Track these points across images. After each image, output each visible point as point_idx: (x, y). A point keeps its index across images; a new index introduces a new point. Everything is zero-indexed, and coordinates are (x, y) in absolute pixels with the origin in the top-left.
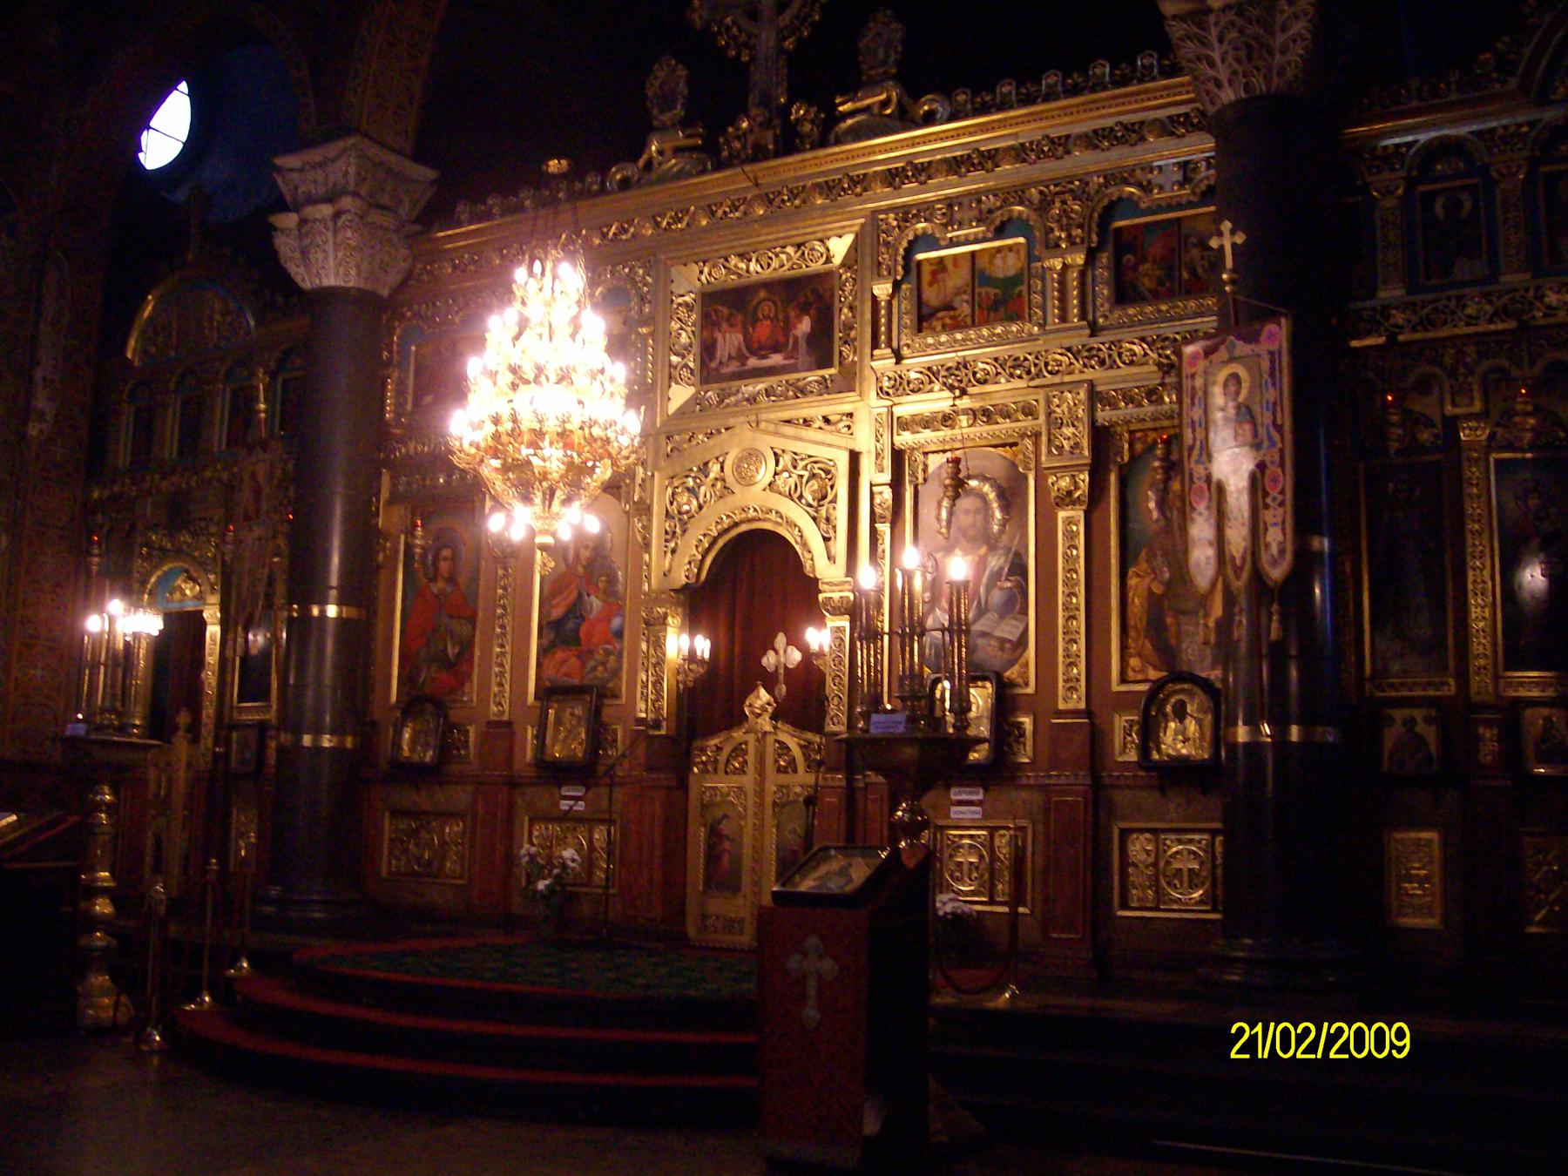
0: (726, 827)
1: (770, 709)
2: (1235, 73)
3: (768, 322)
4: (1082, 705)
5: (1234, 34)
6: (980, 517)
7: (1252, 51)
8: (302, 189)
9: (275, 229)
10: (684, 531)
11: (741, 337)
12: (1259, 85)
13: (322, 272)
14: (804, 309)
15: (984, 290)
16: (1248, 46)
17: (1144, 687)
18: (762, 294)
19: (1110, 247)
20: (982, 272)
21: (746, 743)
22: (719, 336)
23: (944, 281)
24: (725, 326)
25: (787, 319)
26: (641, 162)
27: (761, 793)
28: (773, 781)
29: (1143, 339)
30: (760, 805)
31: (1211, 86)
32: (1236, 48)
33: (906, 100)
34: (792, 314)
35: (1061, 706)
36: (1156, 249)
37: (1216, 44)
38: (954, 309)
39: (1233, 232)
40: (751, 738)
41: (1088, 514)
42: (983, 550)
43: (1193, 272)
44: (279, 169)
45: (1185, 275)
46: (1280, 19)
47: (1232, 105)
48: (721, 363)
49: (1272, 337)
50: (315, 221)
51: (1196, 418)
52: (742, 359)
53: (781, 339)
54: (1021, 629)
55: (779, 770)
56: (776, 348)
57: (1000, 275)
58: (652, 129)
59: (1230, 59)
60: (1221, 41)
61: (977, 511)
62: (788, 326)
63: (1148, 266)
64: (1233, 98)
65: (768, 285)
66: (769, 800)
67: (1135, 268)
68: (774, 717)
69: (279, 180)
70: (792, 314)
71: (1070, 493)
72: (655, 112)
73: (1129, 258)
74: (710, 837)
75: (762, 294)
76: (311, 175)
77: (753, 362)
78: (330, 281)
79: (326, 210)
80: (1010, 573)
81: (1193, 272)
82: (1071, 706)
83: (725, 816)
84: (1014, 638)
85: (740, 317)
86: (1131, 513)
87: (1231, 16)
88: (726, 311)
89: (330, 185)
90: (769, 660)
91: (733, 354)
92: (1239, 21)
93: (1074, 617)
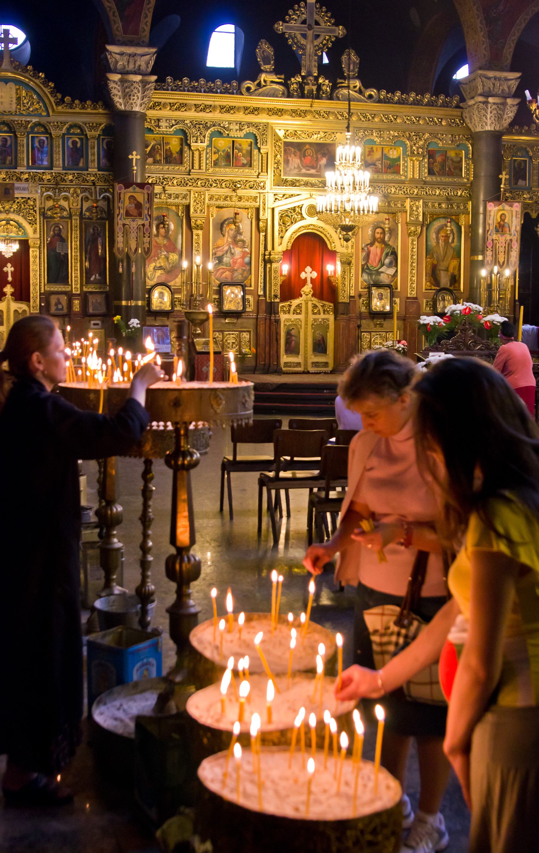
0: (293, 332)
1: (312, 293)
2: (493, 123)
3: (309, 157)
4: (415, 296)
5: (495, 112)
6: (382, 236)
7: (499, 118)
8: (120, 63)
9: (109, 80)
10: (287, 230)
11: (299, 161)
12: (497, 128)
13: (134, 105)
14: (324, 155)
15: (386, 161)
16: (499, 117)
17: (434, 291)
18: (307, 146)
19: (427, 156)
20: (385, 155)
21: (301, 304)
22: (290, 158)
23: (373, 155)
24: (293, 155)
25: (317, 158)
26: (256, 83)
27: (306, 321)
28: (311, 317)
29: (439, 188)
30: (306, 324)
31: (484, 124)
32: (495, 117)
33: (362, 88)
34: (319, 156)
35: (409, 296)
36: (439, 159)
37: (489, 113)
38: (376, 165)
39: (506, 175)
40: (303, 302)
41: (418, 238)
42: (383, 246)
43: (450, 169)
44: (108, 51)
45: (447, 169)
46: (506, 111)
47: (488, 131)
48: (291, 169)
49: (517, 206)
50: (134, 82)
51: (490, 223)
52: (300, 170)
53: (315, 165)
54: (395, 271)
55: (314, 314)
56: (313, 167)
57: (391, 157)
58: (262, 71)
59: (493, 118)
60: (491, 113)
61: (381, 233)
62: (317, 160)
63: (436, 164)
64: (489, 129)
65: (310, 144)
66: (310, 323)
67: (433, 164)
68: (313, 295)
69: (109, 57)
70: (319, 156)
71: (414, 232)
72: (262, 63)
73: (431, 160)
74: (287, 336)
75: (307, 146)
76: (126, 58)
77: (304, 171)
78: (137, 109)
79: (138, 78)
80: (392, 254)
81: (450, 169)
82: (411, 296)
83: (293, 329)
84: (392, 274)
85: (298, 153)
86: (428, 239)
87: (494, 107)
88: (293, 149)
89: (137, 65)
90: (303, 275)
91: (296, 166)
92: (498, 109)
93: (413, 270)
